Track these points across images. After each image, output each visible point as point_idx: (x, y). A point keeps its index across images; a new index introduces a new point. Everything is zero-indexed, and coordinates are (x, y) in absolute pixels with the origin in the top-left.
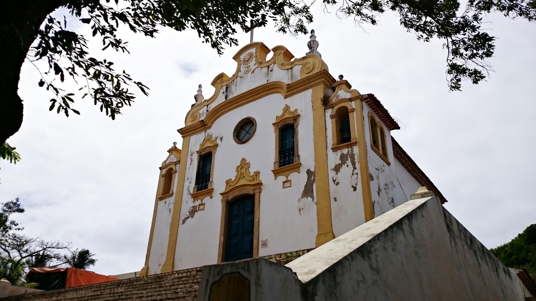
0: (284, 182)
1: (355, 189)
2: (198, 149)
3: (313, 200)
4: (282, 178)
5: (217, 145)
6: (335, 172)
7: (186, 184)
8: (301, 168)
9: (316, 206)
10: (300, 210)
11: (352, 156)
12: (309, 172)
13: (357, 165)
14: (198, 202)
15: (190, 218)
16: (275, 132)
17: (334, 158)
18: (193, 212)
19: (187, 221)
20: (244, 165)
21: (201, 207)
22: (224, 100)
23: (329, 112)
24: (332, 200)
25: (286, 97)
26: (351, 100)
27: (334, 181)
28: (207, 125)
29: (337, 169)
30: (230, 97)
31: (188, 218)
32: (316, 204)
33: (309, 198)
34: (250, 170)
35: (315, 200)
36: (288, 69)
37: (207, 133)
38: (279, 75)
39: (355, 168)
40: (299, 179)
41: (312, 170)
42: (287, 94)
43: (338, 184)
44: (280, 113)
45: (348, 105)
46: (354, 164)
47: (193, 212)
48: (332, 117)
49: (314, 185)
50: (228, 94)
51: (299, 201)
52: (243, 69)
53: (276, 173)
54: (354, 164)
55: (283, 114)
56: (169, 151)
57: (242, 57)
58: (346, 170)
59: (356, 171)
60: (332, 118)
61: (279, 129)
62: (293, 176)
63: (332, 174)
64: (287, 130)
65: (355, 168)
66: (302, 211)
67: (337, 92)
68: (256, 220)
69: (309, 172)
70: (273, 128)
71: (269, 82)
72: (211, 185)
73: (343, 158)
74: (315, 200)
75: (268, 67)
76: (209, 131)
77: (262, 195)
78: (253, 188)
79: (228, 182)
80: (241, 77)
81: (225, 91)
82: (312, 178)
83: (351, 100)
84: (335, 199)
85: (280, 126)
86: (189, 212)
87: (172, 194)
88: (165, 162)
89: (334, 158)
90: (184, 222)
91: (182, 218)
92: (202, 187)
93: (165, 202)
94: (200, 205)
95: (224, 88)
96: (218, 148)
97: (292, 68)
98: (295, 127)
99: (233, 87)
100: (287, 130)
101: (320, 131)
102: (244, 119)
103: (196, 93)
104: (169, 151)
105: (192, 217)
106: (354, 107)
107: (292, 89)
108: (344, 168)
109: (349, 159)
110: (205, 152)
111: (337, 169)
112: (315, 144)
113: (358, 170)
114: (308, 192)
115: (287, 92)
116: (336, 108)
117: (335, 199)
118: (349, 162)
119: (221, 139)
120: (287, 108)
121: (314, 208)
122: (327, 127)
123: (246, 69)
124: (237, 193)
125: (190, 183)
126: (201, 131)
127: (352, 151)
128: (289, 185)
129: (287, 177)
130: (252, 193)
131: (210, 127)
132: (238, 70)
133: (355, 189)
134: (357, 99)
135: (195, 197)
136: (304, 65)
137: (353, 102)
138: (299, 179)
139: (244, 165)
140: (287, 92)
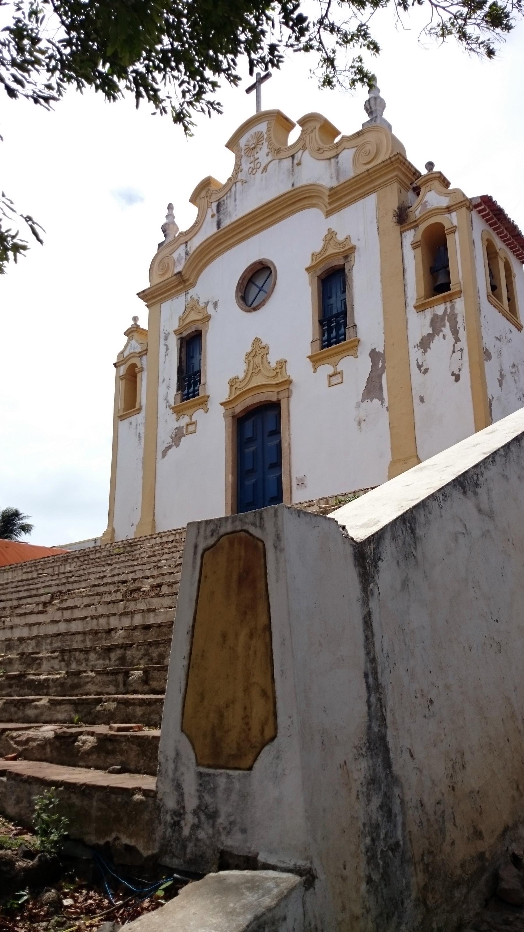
0: (330, 376)
1: (457, 378)
2: (176, 327)
3: (382, 404)
4: (326, 369)
5: (208, 318)
6: (421, 350)
7: (162, 390)
8: (360, 348)
9: (387, 413)
10: (359, 423)
11: (453, 318)
12: (374, 355)
13: (462, 334)
14: (184, 421)
15: (174, 448)
16: (311, 283)
18: (178, 437)
19: (170, 452)
20: (258, 350)
21: (191, 428)
22: (215, 230)
23: (410, 237)
24: (416, 401)
25: (328, 214)
27: (419, 367)
28: (188, 280)
29: (425, 344)
30: (226, 222)
31: (170, 447)
32: (387, 410)
33: (376, 401)
34: (270, 358)
35: (386, 404)
36: (329, 159)
37: (189, 296)
38: (316, 172)
39: (457, 340)
42: (329, 208)
43: (426, 371)
44: (318, 247)
45: (444, 219)
46: (455, 332)
47: (178, 437)
48: (415, 246)
49: (384, 376)
50: (221, 216)
51: (358, 406)
52: (246, 166)
53: (316, 360)
54: (455, 332)
55: (324, 249)
56: (127, 333)
57: (242, 142)
58: (442, 345)
59: (459, 346)
60: (414, 248)
62: (346, 364)
63: (415, 354)
64: (332, 280)
65: (457, 340)
66: (363, 424)
67: (424, 195)
68: (284, 445)
69: (374, 355)
70: (306, 277)
71: (296, 186)
72: (205, 389)
73: (436, 324)
74: (386, 404)
75: (293, 157)
76: (192, 292)
77: (293, 400)
78: (277, 390)
79: (232, 383)
80: (244, 182)
81: (215, 211)
82: (381, 364)
83: (449, 209)
84: (422, 399)
85: (319, 273)
86: (172, 438)
87: (140, 409)
88: (122, 353)
89: (418, 325)
90: (164, 454)
91: (161, 448)
92: (188, 393)
93: (131, 423)
94: (188, 425)
95: (214, 205)
96: (211, 323)
97: (337, 156)
98: (347, 271)
99: (230, 204)
100: (332, 280)
101: (392, 275)
102: (255, 264)
103: (164, 221)
104: (127, 333)
105: (177, 446)
106: (455, 223)
107: (339, 198)
108: (437, 342)
109: (448, 324)
110: (189, 332)
111: (425, 344)
112: (385, 301)
113: (463, 344)
114: (372, 389)
115: (330, 204)
116: (422, 227)
117: (422, 399)
118: (447, 330)
119: (215, 305)
121: (385, 416)
122: (406, 266)
123: (252, 165)
124: (250, 401)
125: (168, 387)
126: (178, 292)
127: (453, 307)
128: (340, 381)
129: (335, 366)
130: (274, 399)
131: (193, 285)
133: (457, 378)
134: (461, 207)
135: (178, 411)
136: (360, 148)
137: (454, 214)
138: (356, 368)
139: (258, 350)
140: (330, 204)
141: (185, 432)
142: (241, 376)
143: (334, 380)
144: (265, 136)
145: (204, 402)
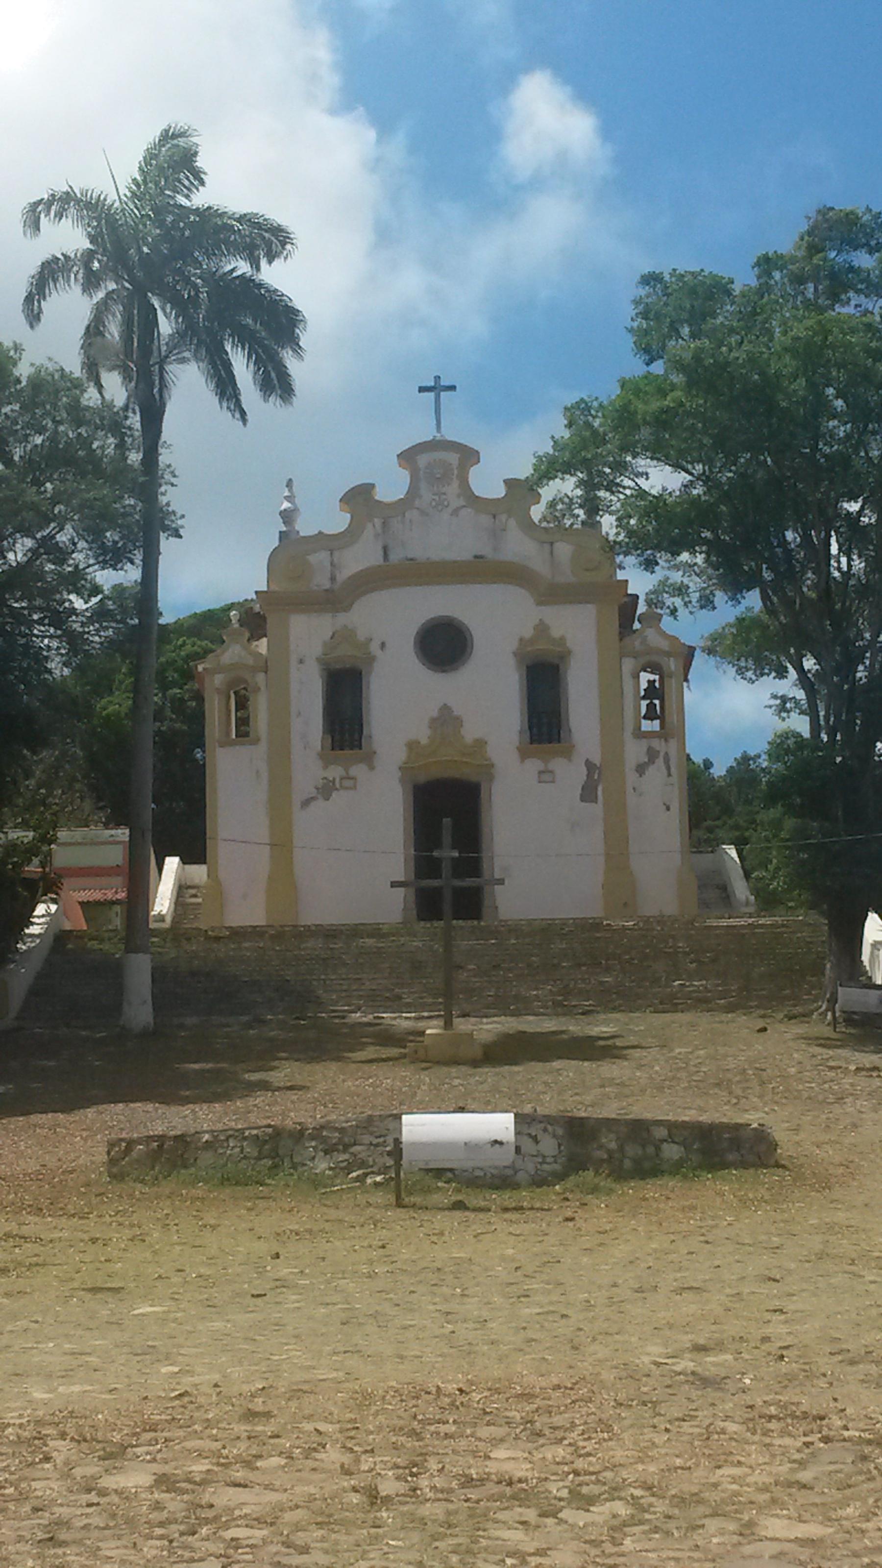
1: (668, 809)
4: (534, 765)
12: (589, 765)
13: (673, 770)
14: (335, 772)
17: (634, 752)
18: (326, 790)
19: (313, 804)
20: (446, 721)
21: (348, 783)
26: (668, 654)
29: (641, 769)
31: (313, 799)
39: (669, 775)
40: (571, 774)
41: (597, 760)
44: (528, 633)
46: (668, 768)
49: (600, 788)
52: (426, 495)
53: (524, 754)
54: (668, 768)
57: (423, 460)
61: (528, 667)
62: (558, 765)
65: (669, 775)
69: (589, 765)
70: (512, 662)
79: (412, 746)
83: (668, 654)
95: (378, 522)
108: (651, 771)
113: (675, 778)
119: (383, 645)
120: (542, 628)
123: (437, 498)
131: (347, 609)
132: (413, 491)
133: (668, 809)
138: (571, 774)
141: (338, 786)
142: (424, 741)
143: (545, 777)
144: (456, 472)
145: (369, 759)
